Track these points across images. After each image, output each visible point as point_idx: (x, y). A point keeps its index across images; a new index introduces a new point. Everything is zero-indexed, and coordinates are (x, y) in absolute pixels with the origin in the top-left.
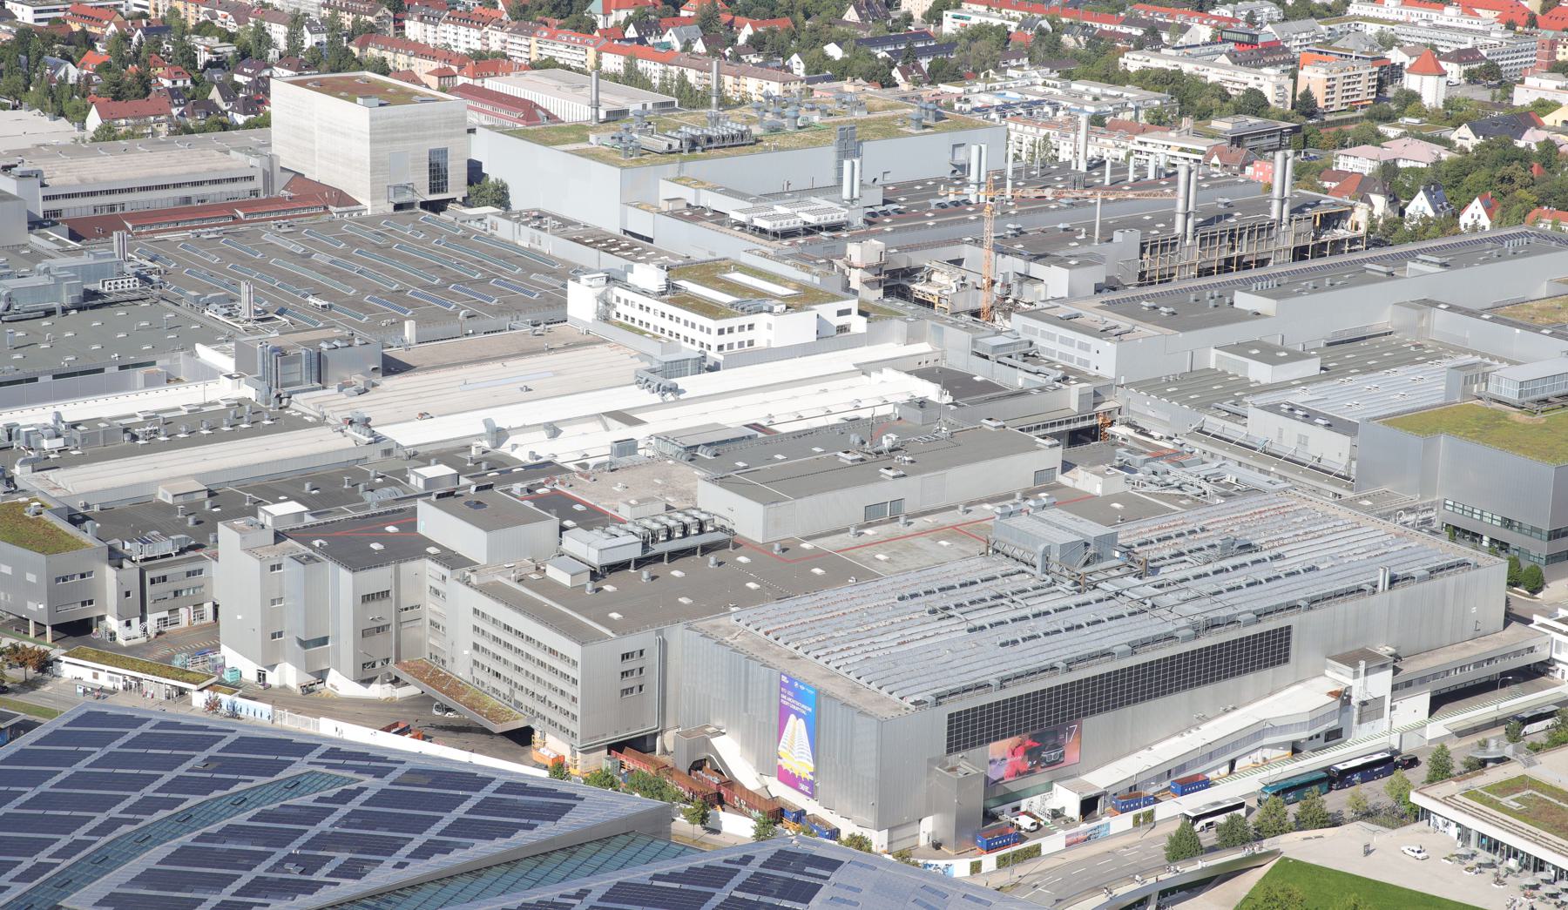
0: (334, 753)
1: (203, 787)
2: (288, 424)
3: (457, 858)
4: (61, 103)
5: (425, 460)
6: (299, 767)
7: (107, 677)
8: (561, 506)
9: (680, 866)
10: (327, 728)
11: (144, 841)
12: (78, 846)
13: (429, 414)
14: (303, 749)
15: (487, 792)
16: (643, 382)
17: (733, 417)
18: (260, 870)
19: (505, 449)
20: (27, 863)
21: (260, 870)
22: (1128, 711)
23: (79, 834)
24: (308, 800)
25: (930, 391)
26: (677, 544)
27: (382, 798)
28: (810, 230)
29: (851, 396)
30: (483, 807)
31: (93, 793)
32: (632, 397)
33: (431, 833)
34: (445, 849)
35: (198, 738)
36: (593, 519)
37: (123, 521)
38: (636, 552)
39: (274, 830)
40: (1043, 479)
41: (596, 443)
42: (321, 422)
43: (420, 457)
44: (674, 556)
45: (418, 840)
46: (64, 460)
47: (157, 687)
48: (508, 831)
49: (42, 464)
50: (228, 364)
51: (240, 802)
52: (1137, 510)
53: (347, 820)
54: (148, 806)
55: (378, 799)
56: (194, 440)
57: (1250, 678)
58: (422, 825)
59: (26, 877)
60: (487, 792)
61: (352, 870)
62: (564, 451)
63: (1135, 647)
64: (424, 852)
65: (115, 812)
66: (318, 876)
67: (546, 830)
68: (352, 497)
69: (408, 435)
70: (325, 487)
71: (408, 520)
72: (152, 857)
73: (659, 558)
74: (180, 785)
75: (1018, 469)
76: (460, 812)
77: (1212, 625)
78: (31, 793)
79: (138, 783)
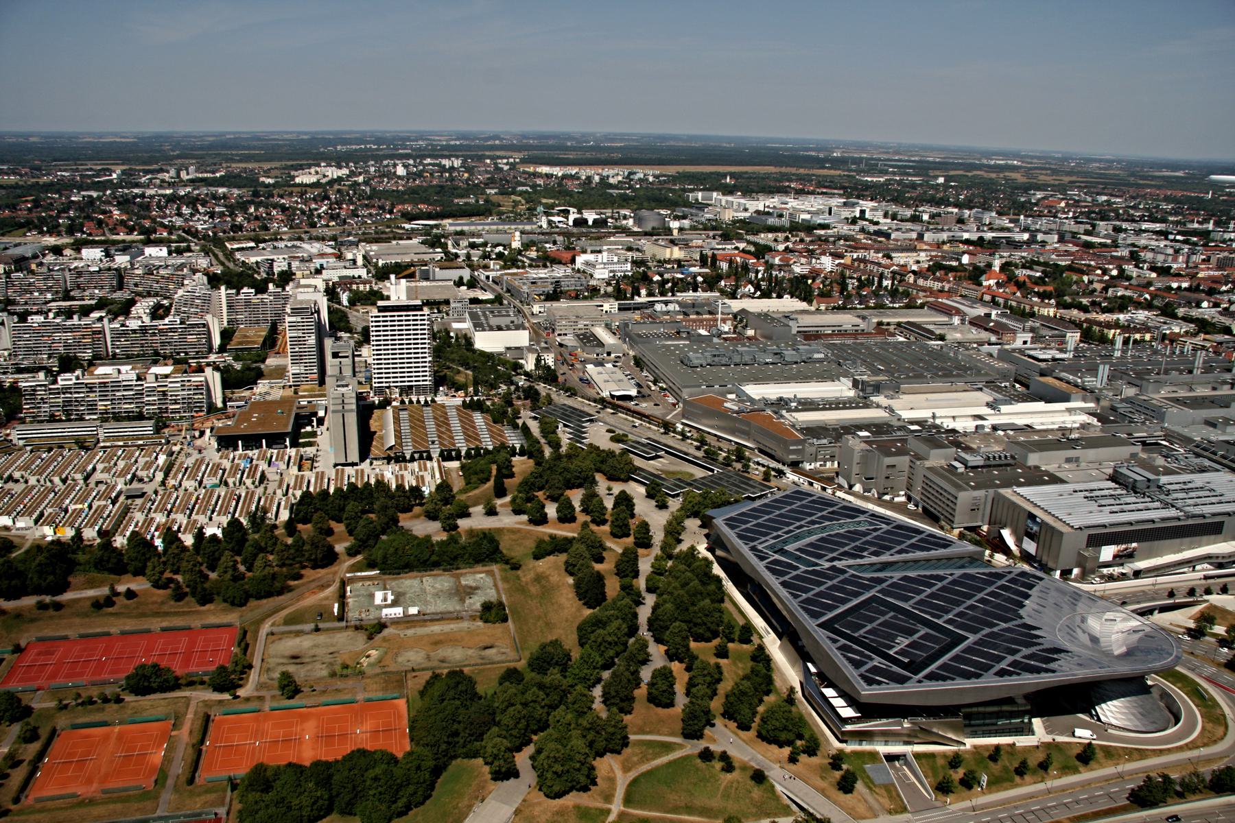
0: (873, 515)
1: (831, 519)
2: (866, 406)
3: (910, 556)
4: (807, 298)
5: (912, 423)
6: (862, 518)
7: (802, 480)
8: (957, 444)
9: (987, 571)
10: (871, 506)
11: (810, 533)
12: (790, 531)
13: (913, 407)
14: (864, 512)
15: (922, 536)
16: (988, 405)
17: (1020, 421)
18: (846, 549)
19: (938, 422)
20: (775, 534)
21: (846, 549)
22: (1156, 543)
23: (791, 528)
24: (863, 529)
25: (1094, 421)
26: (998, 462)
27: (887, 532)
28: (1054, 360)
29: (1062, 419)
30: (921, 540)
31: (798, 515)
32: (985, 411)
33: (903, 546)
34: (907, 552)
35: (830, 503)
36: (968, 449)
37: (814, 431)
38: (981, 463)
39: (853, 535)
40: (1134, 456)
41: (970, 425)
42: (878, 406)
43: (912, 423)
44: (995, 466)
45: (899, 548)
46: (796, 410)
47: (817, 486)
48: (929, 549)
49: (789, 410)
50: (850, 384)
51: (841, 526)
52: (1168, 472)
53: (875, 538)
54: (813, 523)
55: (886, 532)
56: (837, 408)
57: (1205, 538)
58: (901, 543)
59: (774, 538)
60: (922, 536)
61: (876, 554)
62: (959, 425)
63: (1163, 520)
64: (899, 552)
65: (802, 523)
66: (865, 554)
67: (941, 552)
68: (887, 433)
69: (906, 415)
70: (878, 428)
71: (904, 441)
72: (813, 538)
73: (989, 466)
74: (822, 517)
75: (1125, 451)
76: (913, 541)
77: (1194, 516)
78: (778, 512)
79: (811, 515)
